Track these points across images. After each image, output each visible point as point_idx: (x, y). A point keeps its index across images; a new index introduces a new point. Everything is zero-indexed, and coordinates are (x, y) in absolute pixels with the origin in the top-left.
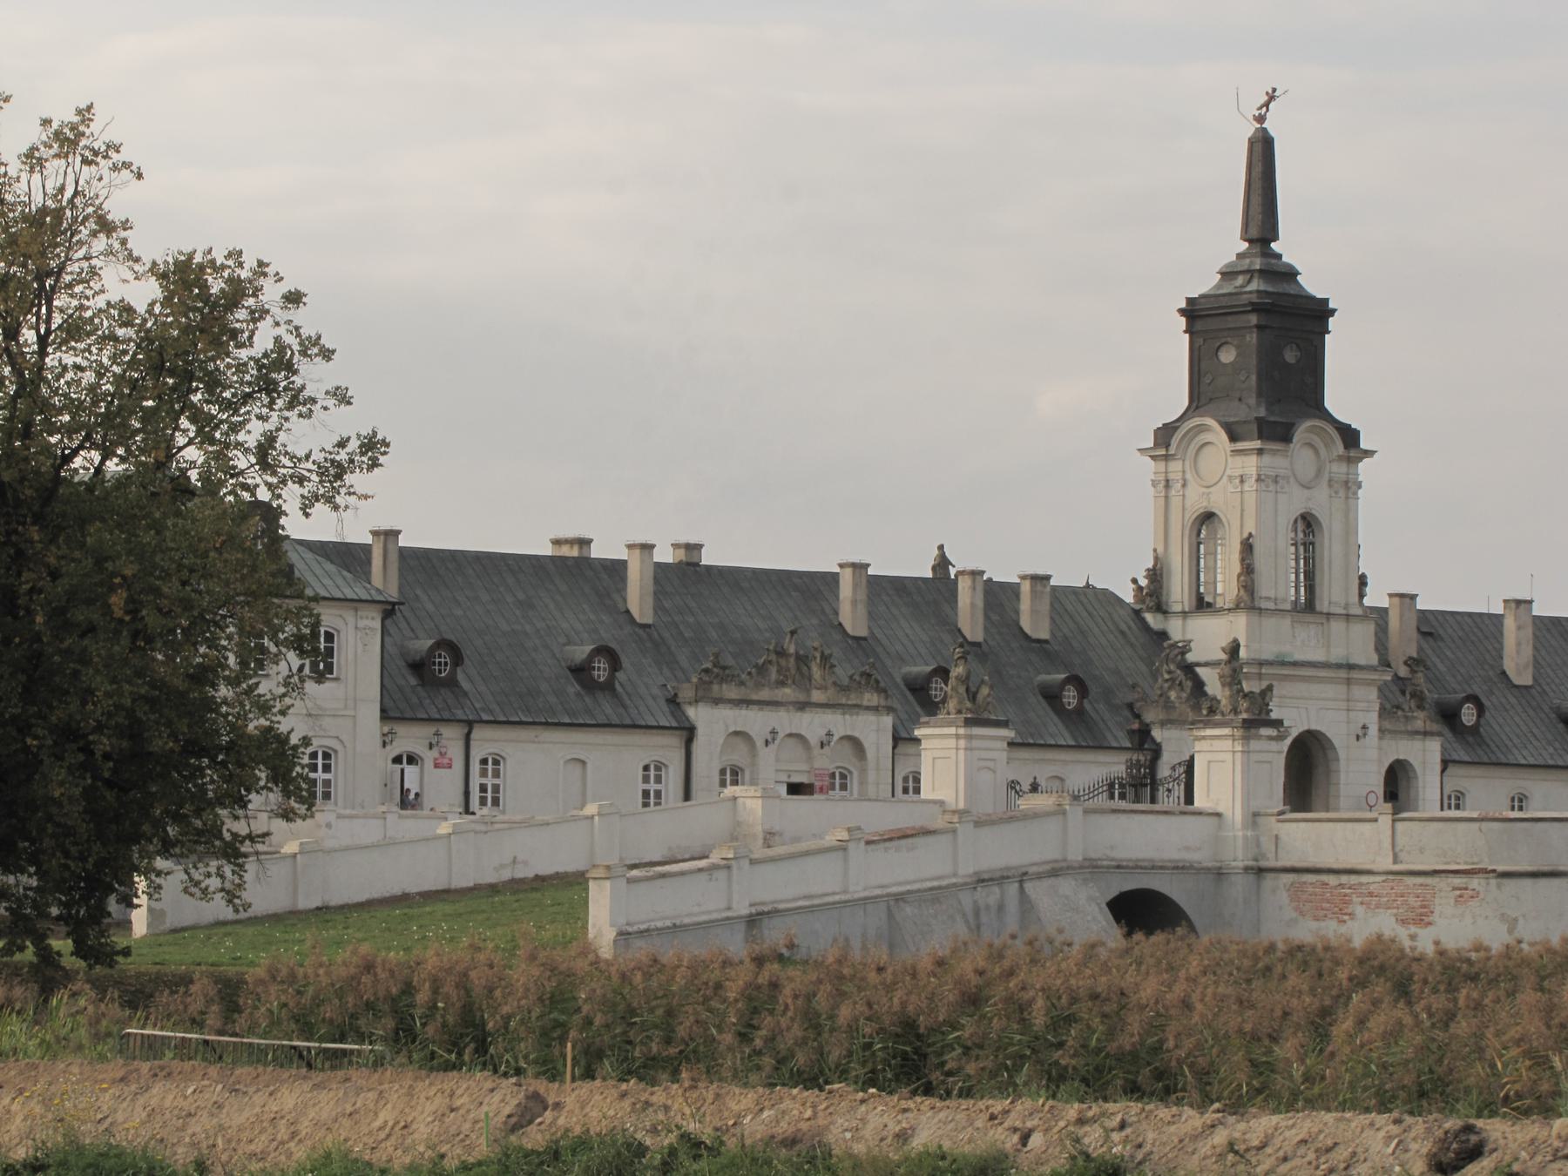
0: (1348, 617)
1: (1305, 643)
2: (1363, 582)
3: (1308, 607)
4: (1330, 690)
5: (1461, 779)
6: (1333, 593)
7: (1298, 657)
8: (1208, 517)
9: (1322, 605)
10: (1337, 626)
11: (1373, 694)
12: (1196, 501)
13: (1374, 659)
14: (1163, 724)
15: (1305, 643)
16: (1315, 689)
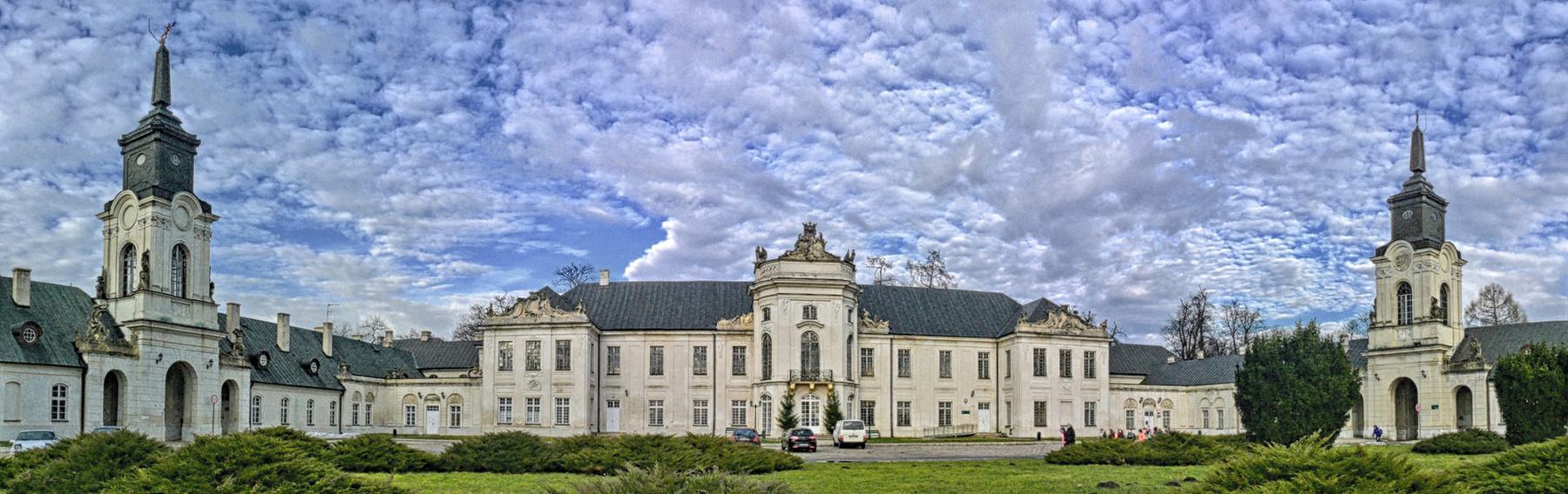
0: (203, 303)
1: (180, 315)
2: (212, 286)
3: (184, 297)
4: (192, 341)
5: (260, 391)
6: (195, 289)
7: (175, 320)
8: (129, 248)
9: (190, 296)
10: (196, 307)
11: (216, 344)
12: (122, 238)
13: (217, 327)
14: (89, 352)
15: (180, 315)
16: (185, 340)
